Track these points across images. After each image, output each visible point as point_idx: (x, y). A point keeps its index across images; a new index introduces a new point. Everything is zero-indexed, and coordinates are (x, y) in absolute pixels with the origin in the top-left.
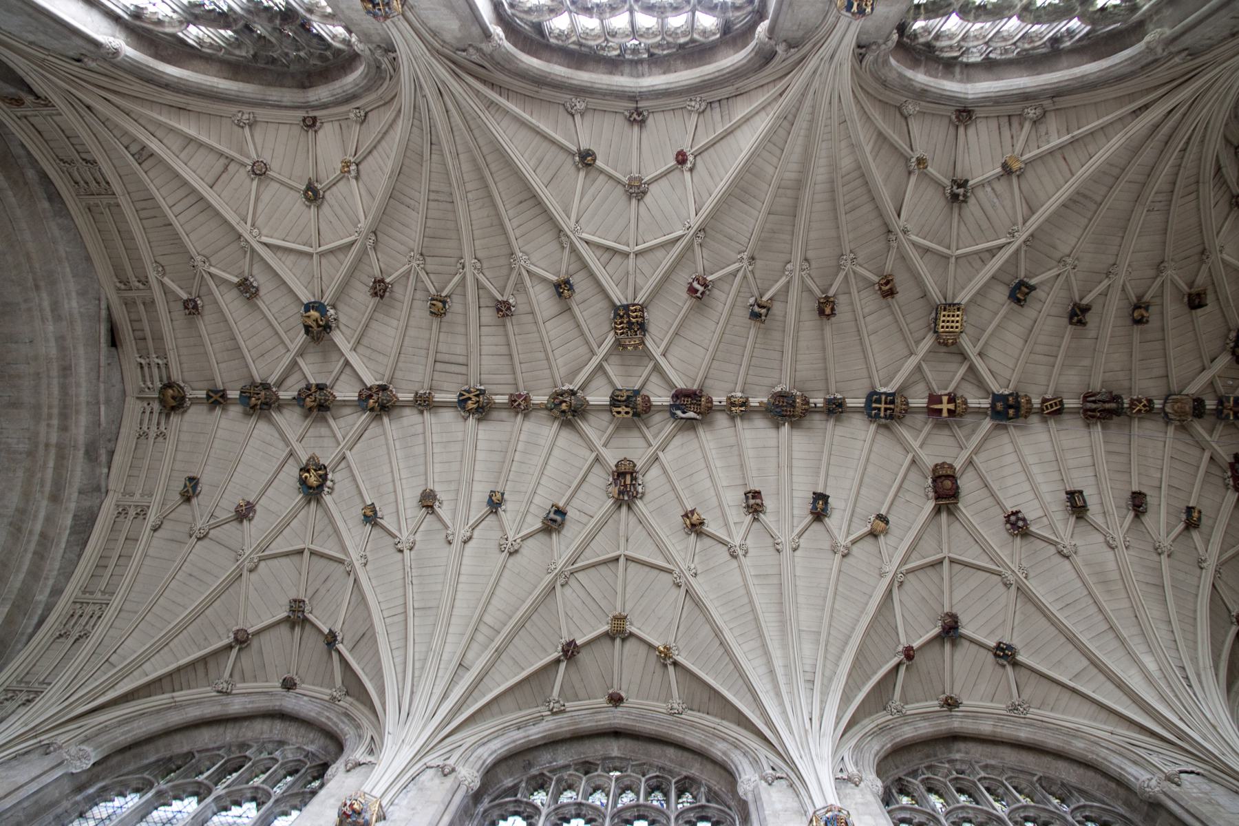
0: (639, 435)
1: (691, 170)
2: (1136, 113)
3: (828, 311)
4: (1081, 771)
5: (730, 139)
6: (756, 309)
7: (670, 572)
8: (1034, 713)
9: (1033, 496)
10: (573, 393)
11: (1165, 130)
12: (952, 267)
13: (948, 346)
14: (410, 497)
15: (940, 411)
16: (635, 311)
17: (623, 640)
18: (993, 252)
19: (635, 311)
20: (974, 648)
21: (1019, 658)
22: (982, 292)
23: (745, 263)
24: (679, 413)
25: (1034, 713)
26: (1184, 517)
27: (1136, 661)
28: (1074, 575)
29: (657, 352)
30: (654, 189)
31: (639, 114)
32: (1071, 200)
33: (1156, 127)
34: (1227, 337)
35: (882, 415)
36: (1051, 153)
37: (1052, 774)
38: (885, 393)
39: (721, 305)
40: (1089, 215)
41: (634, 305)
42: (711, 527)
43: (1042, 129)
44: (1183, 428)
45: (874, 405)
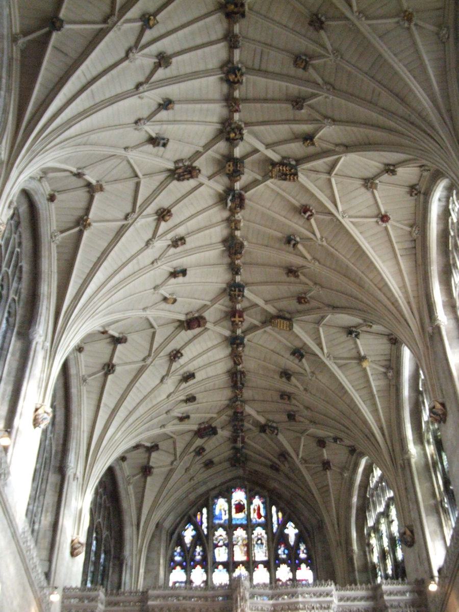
0: (215, 172)
1: (377, 222)
2: (381, 429)
4: (63, 422)
7: (133, 211)
8: (84, 389)
10: (242, 139)
11: (372, 439)
12: (312, 326)
14: (167, 45)
15: (235, 317)
16: (294, 179)
17: (88, 192)
18: (320, 345)
21: (110, 377)
22: (297, 336)
23: (319, 242)
24: (230, 197)
25: (84, 389)
26: (184, 415)
29: (269, 182)
30: (368, 194)
31: (416, 194)
32: (343, 388)
34: (273, 422)
35: (232, 293)
36: (368, 381)
38: (243, 291)
39: (295, 221)
41: (297, 178)
42: (163, 226)
43: (381, 377)
44: (228, 406)
45: (237, 289)
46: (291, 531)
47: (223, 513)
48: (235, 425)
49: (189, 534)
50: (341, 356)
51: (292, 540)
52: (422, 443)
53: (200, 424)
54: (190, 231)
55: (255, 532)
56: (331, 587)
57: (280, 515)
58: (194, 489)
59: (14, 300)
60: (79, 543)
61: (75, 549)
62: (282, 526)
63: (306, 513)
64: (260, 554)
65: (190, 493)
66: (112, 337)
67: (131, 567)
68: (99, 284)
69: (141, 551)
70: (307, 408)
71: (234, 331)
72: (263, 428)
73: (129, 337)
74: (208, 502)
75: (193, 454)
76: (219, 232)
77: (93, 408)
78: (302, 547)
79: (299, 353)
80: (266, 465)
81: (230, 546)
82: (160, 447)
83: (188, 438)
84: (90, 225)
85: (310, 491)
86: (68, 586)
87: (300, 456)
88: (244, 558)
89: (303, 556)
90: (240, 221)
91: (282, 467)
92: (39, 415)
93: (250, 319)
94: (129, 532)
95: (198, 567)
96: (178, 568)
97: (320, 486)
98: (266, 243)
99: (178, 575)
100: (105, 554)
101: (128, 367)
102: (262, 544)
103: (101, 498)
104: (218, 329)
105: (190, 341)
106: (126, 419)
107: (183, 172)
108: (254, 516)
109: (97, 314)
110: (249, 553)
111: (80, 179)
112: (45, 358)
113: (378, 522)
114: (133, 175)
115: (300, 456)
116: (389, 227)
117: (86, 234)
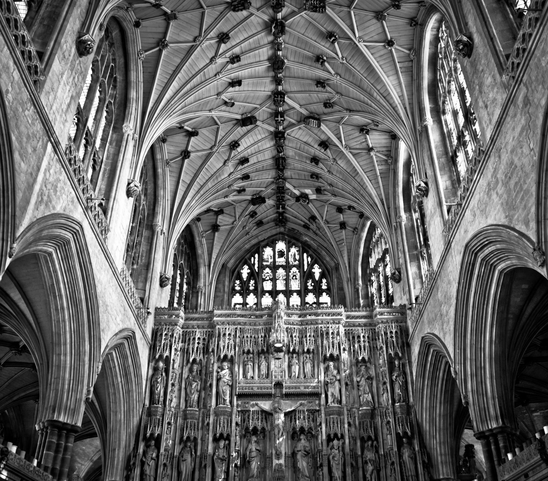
1: (384, 46)
3: (319, 85)
4: (152, 193)
5: (394, 72)
6: (321, 61)
8: (167, 169)
9: (246, 147)
13: (305, 120)
16: (322, 11)
17: (165, 19)
18: (339, 139)
19: (322, 11)
20: (186, 142)
21: (186, 161)
22: (323, 132)
23: (341, 61)
24: (274, 25)
25: (167, 169)
26: (241, 189)
27: (193, 198)
28: (218, 168)
29: (303, 13)
30: (379, 24)
31: (415, 25)
33: (377, 206)
37: (149, 182)
38: (284, 98)
39: (323, 44)
40: (351, 173)
41: (325, 10)
42: (223, 47)
43: (383, 163)
44: (273, 182)
46: (317, 271)
47: (270, 258)
48: (279, 196)
49: (245, 272)
50: (355, 147)
51: (317, 276)
52: (410, 211)
53: (253, 195)
54: (244, 50)
55: (292, 271)
56: (342, 310)
57: (309, 259)
58: (249, 240)
59: (110, 102)
60: (166, 278)
61: (163, 282)
62: (311, 266)
63: (328, 259)
64: (295, 285)
65: (246, 244)
66: (187, 131)
67: (205, 294)
68: (175, 91)
69: (211, 283)
70: (330, 185)
71: (277, 128)
72: (298, 199)
73: (200, 131)
74: (258, 249)
75: (248, 216)
76: (265, 53)
77: (174, 183)
78: (324, 281)
79: (325, 144)
80: (300, 225)
81: (274, 280)
82: (225, 211)
83: (244, 205)
84: (167, 45)
85: (331, 243)
86: (159, 307)
87: (324, 219)
88: (284, 289)
89: (324, 287)
90: (281, 44)
91: (311, 226)
92: (131, 187)
93: (289, 119)
94: (202, 270)
95: (252, 294)
96: (238, 295)
97: (337, 240)
98: (301, 61)
99: (237, 299)
100: (187, 284)
101: (199, 154)
102: (296, 279)
103: (183, 247)
104: (266, 126)
105: (245, 134)
106: (198, 192)
107: (238, 4)
108: (291, 260)
109: (174, 113)
110: (287, 284)
111: (158, 10)
112: (135, 146)
113: (377, 266)
114: (199, 6)
115: (324, 219)
116: (393, 50)
117: (164, 52)
